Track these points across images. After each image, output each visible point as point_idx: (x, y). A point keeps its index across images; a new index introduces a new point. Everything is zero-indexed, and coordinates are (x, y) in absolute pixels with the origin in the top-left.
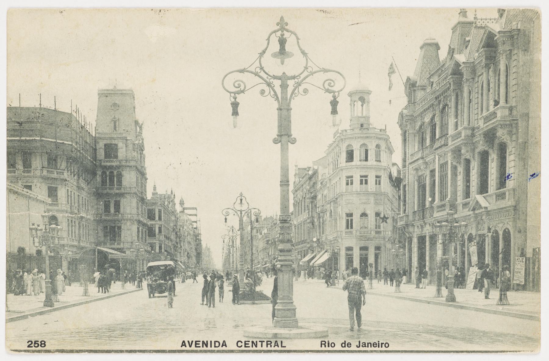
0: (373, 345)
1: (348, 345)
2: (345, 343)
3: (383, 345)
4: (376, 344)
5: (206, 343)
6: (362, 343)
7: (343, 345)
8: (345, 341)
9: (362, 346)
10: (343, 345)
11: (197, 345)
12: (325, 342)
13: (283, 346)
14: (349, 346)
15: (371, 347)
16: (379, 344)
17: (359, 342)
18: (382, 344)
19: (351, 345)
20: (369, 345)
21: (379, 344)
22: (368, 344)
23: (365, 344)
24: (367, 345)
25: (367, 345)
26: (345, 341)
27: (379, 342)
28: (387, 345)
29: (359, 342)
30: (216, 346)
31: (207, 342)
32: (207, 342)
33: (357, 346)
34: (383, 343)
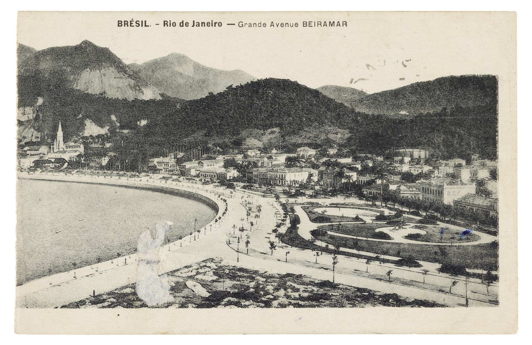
0: (207, 24)
3: (217, 25)
4: (209, 23)
7: (182, 24)
8: (183, 21)
9: (197, 26)
10: (182, 24)
11: (310, 25)
13: (146, 25)
15: (205, 26)
16: (212, 23)
18: (215, 23)
19: (188, 24)
21: (212, 23)
22: (202, 23)
26: (183, 21)
27: (212, 21)
34: (217, 23)
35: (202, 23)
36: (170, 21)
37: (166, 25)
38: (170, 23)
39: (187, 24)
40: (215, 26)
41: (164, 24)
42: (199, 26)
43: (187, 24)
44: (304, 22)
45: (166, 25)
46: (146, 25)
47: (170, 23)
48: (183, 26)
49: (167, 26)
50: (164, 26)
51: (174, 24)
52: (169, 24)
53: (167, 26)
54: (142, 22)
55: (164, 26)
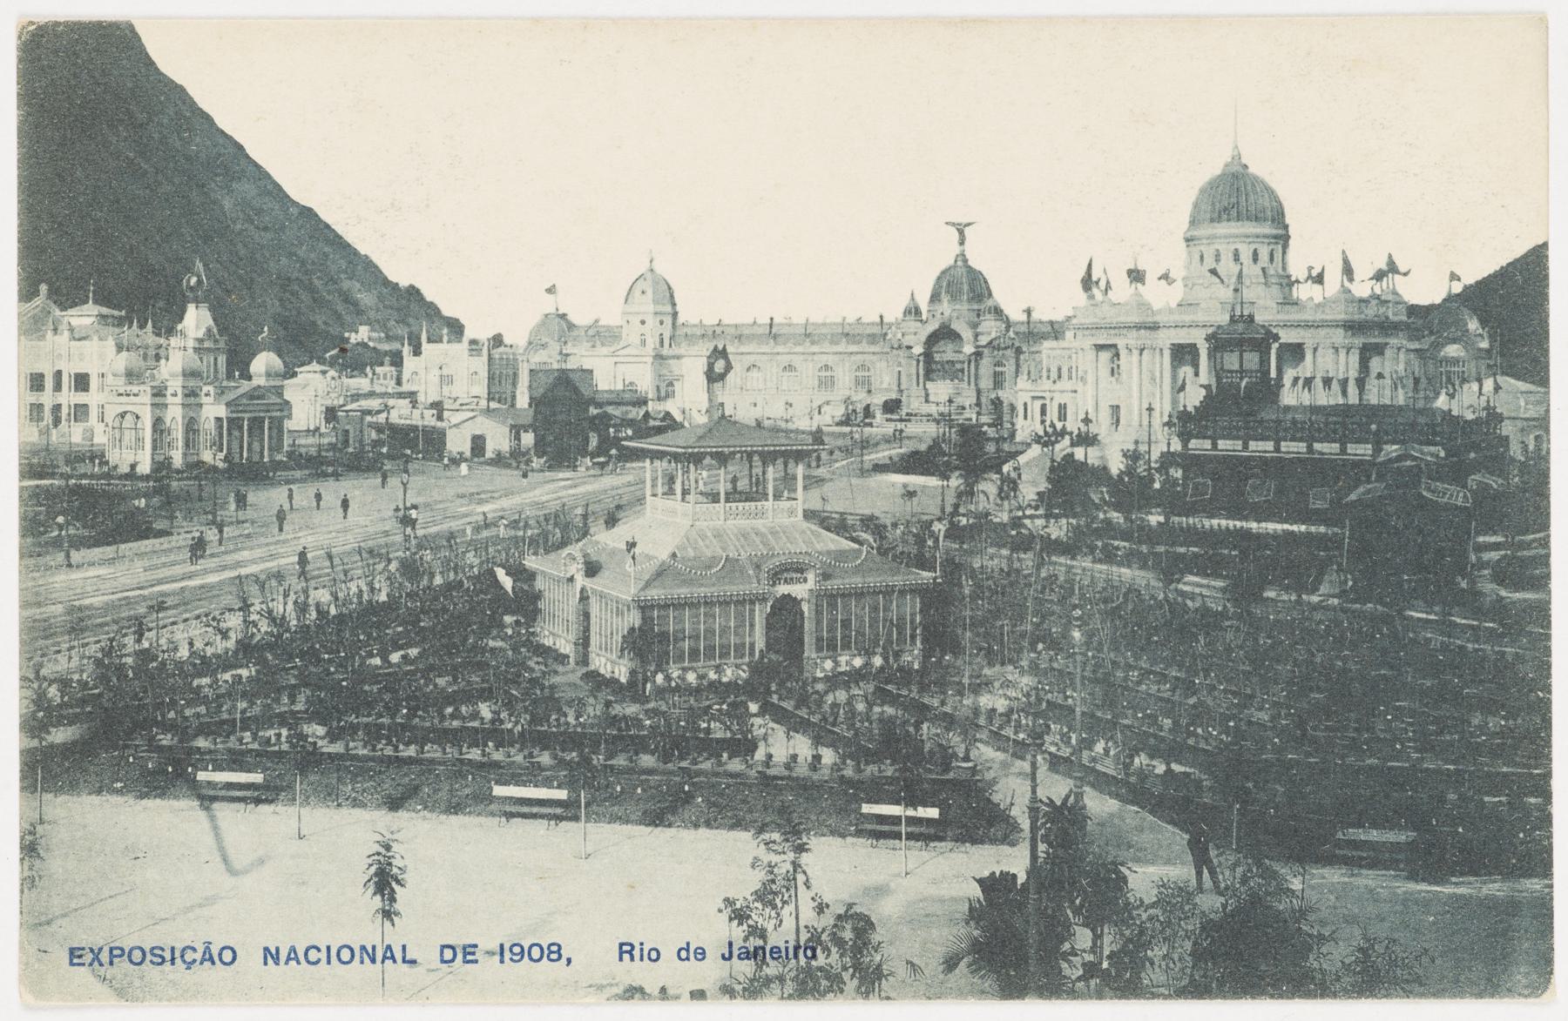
2: (688, 950)
5: (274, 952)
7: (684, 955)
8: (688, 944)
10: (684, 955)
14: (699, 957)
16: (787, 948)
17: (730, 944)
21: (787, 948)
26: (688, 944)
29: (730, 944)
31: (277, 950)
32: (277, 950)
36: (642, 944)
38: (642, 950)
39: (701, 954)
41: (621, 953)
43: (701, 954)
45: (626, 957)
46: (407, 958)
47: (642, 950)
48: (688, 959)
49: (632, 959)
50: (621, 959)
52: (636, 953)
53: (632, 959)
55: (621, 959)
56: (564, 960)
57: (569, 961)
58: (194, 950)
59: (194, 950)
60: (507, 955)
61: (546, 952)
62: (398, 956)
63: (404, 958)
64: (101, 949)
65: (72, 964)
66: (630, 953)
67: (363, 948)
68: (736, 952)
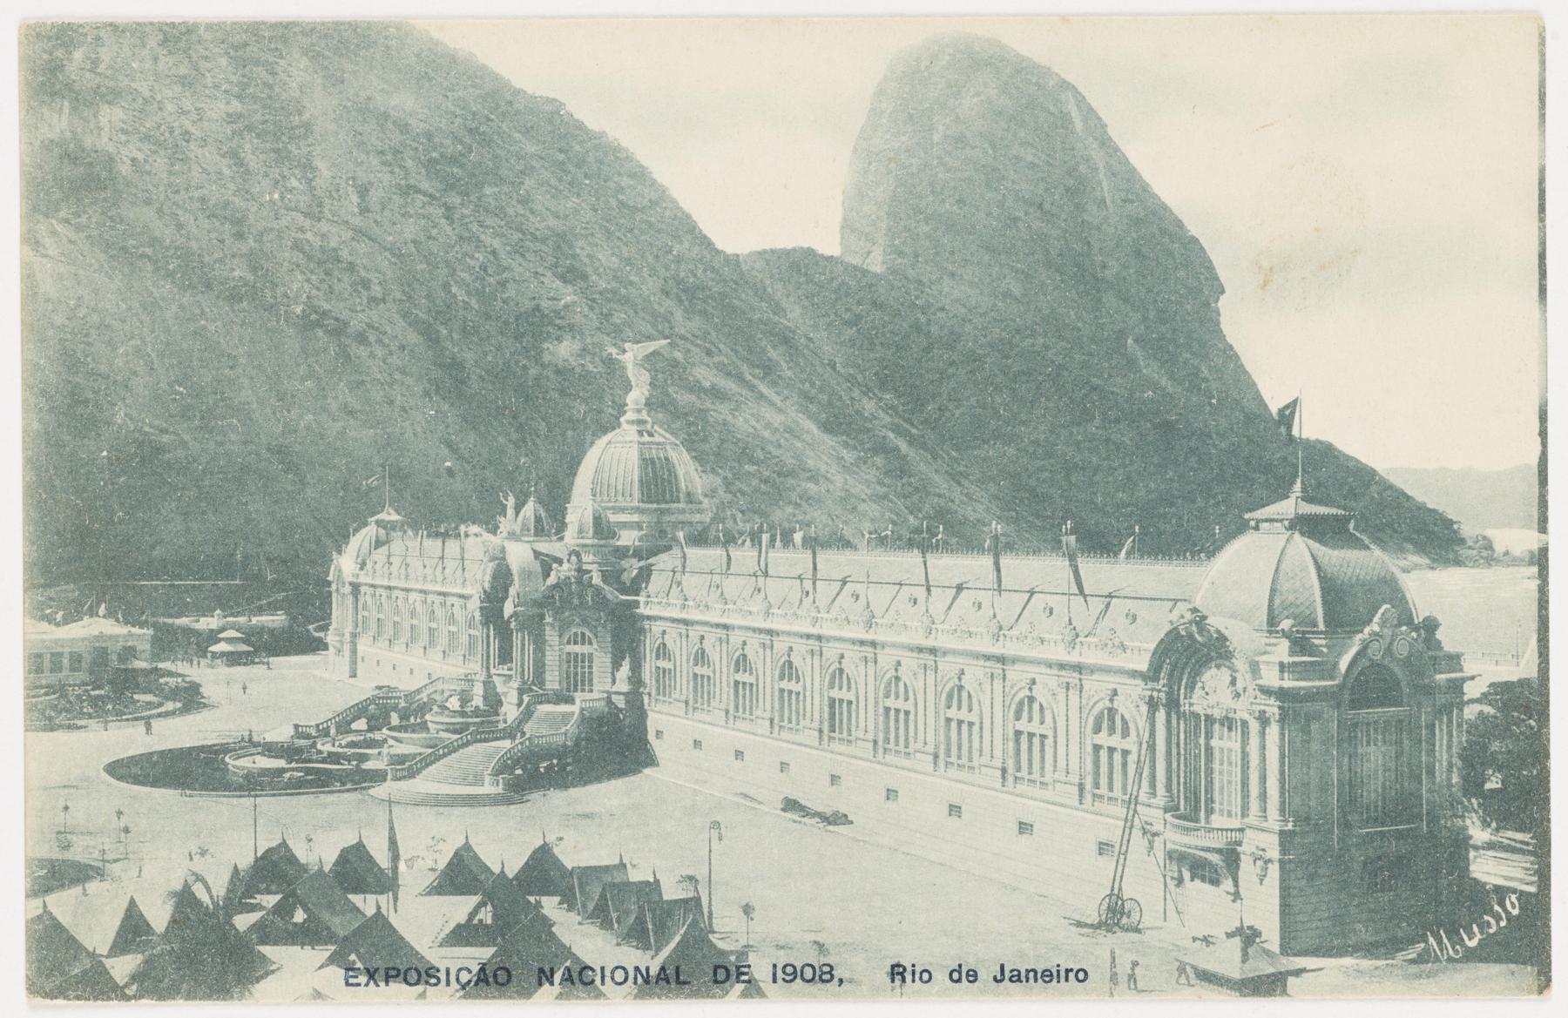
1: (968, 975)
2: (960, 973)
3: (1072, 975)
4: (1051, 975)
6: (1012, 971)
7: (956, 976)
8: (960, 966)
9: (1011, 980)
10: (956, 976)
12: (905, 969)
15: (1036, 980)
17: (1002, 967)
18: (1068, 971)
20: (1031, 974)
23: (1019, 975)
24: (1023, 979)
25: (1023, 979)
26: (960, 966)
28: (1081, 976)
29: (1002, 967)
30: (500, 980)
33: (995, 979)
34: (1072, 970)
35: (1028, 971)
37: (898, 978)
39: (973, 976)
40: (1067, 980)
41: (893, 975)
42: (1019, 980)
44: (388, 969)
45: (898, 978)
48: (959, 981)
49: (904, 980)
51: (926, 976)
52: (908, 977)
54: (603, 969)
56: (836, 980)
57: (841, 981)
58: (470, 971)
59: (470, 971)
60: (780, 974)
61: (818, 973)
62: (673, 979)
63: (678, 977)
64: (377, 970)
65: (347, 984)
66: (902, 974)
67: (637, 969)
68: (1007, 975)
